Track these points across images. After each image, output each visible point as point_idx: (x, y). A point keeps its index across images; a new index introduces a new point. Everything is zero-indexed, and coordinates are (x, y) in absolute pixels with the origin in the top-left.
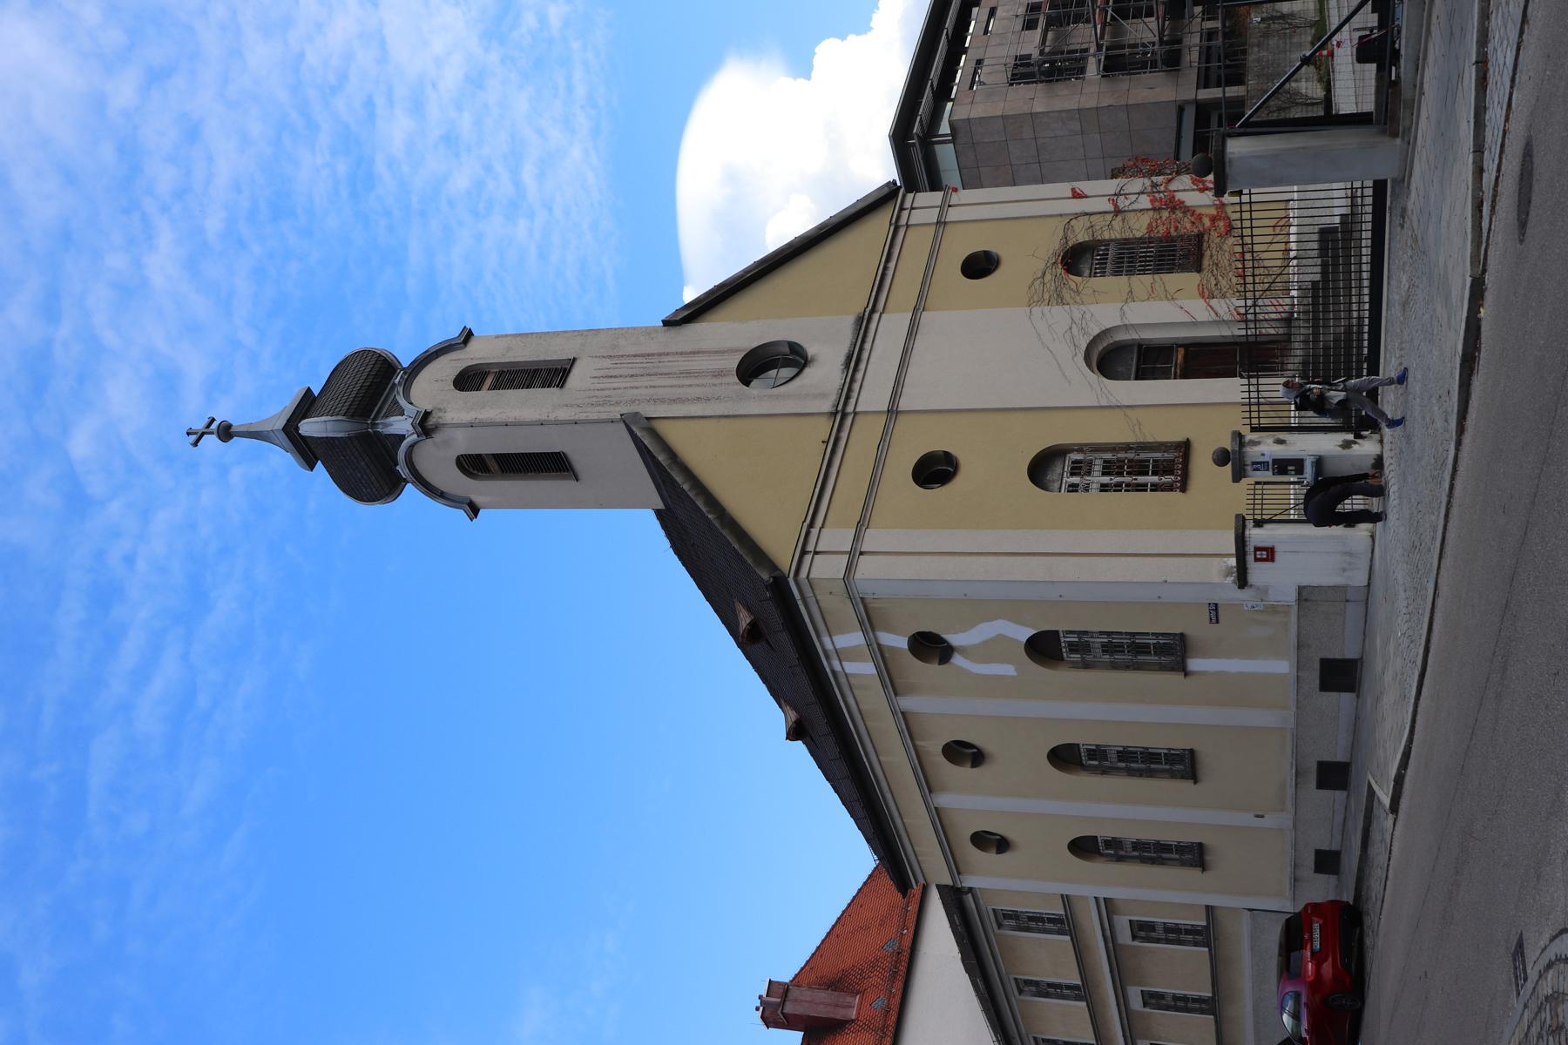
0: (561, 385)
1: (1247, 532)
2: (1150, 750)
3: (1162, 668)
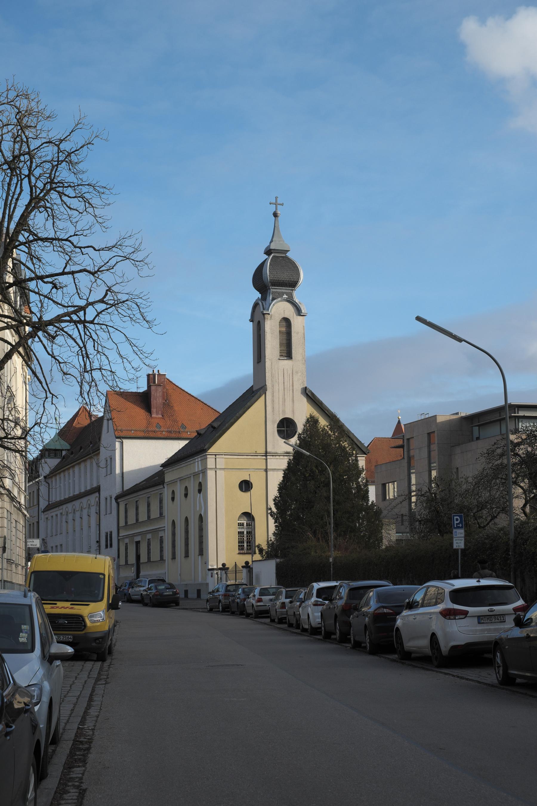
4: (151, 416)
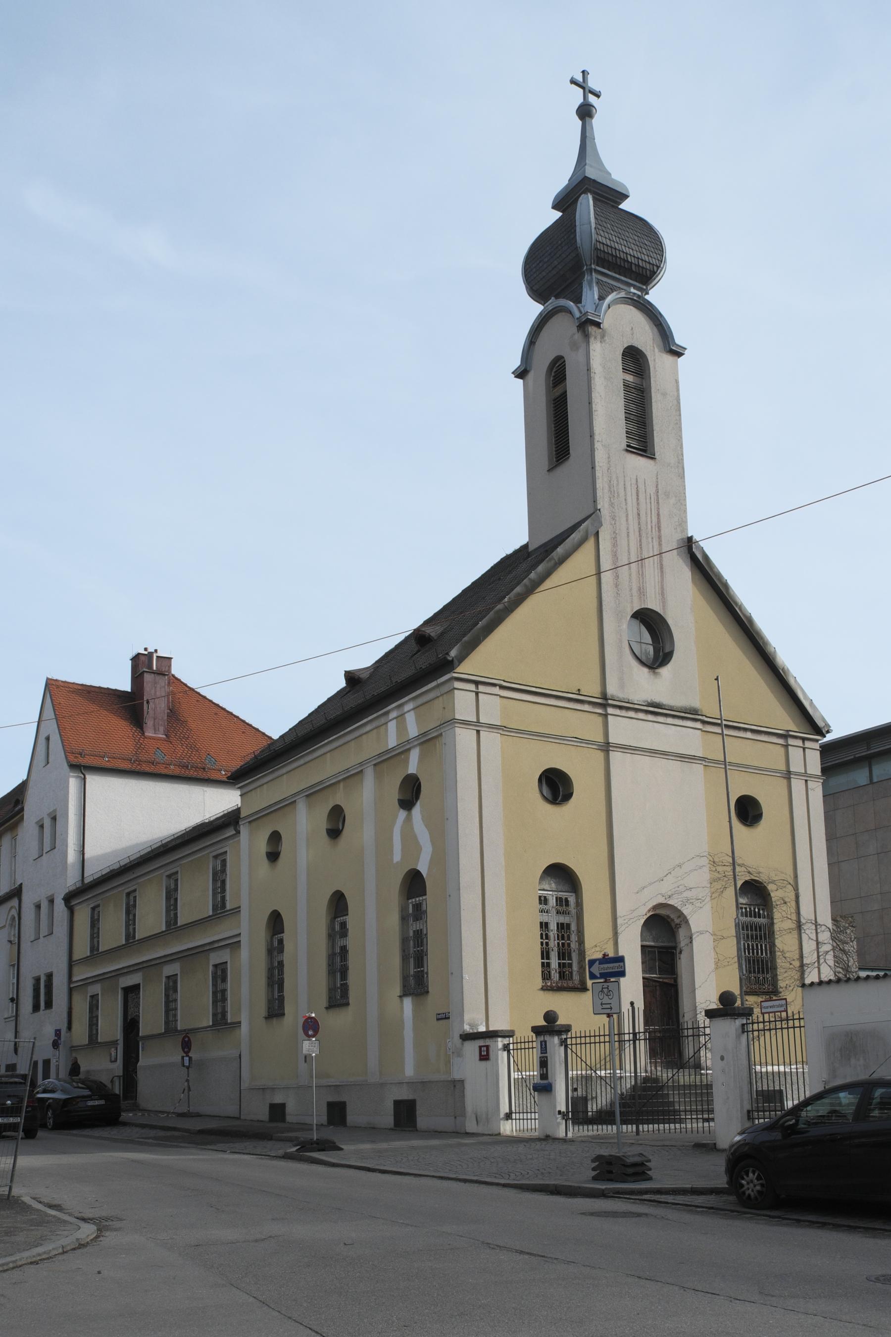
0: (629, 449)
1: (500, 1039)
3: (405, 978)
4: (143, 734)
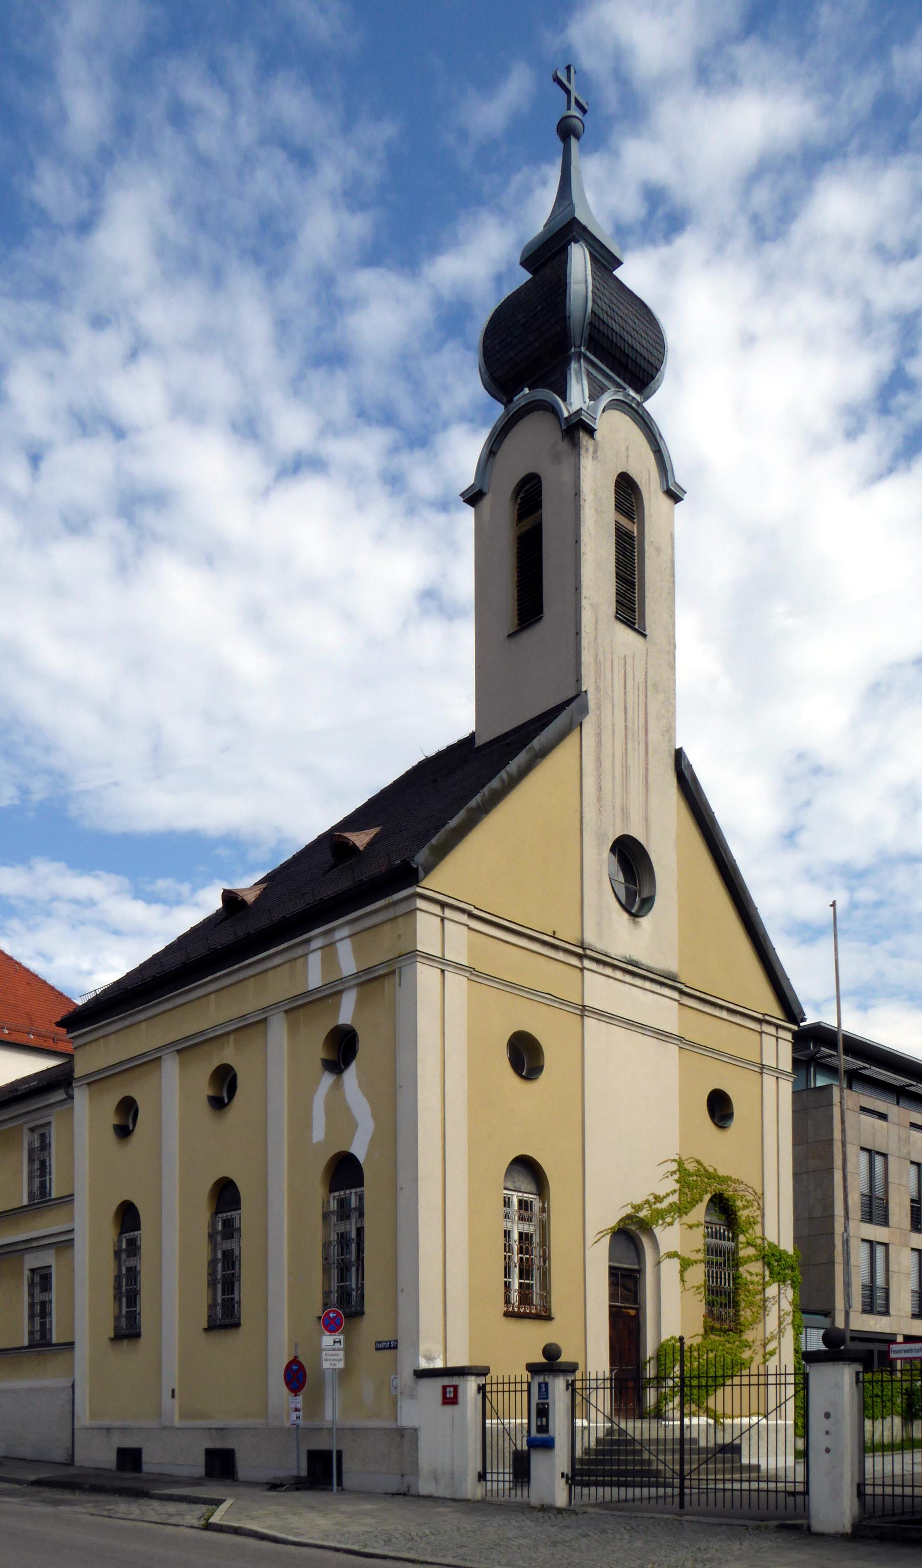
1: (473, 1378)
2: (236, 1284)
